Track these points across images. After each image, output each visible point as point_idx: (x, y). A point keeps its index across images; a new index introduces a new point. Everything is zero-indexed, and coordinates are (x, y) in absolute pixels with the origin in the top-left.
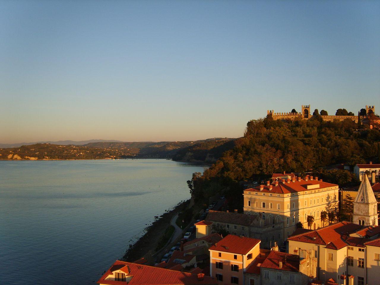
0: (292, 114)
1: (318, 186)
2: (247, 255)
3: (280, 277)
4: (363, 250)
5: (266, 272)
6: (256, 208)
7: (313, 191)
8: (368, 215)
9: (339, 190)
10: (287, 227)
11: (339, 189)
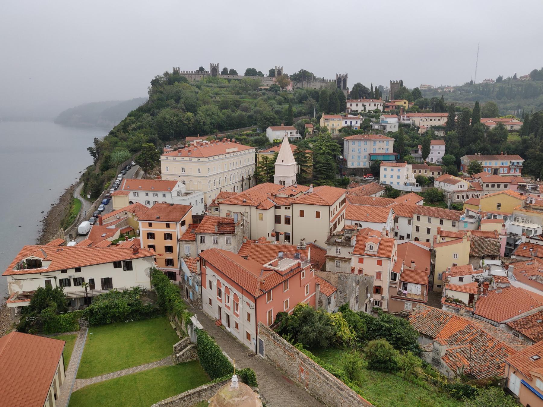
0: (200, 73)
1: (236, 149)
2: (180, 222)
4: (289, 208)
7: (232, 154)
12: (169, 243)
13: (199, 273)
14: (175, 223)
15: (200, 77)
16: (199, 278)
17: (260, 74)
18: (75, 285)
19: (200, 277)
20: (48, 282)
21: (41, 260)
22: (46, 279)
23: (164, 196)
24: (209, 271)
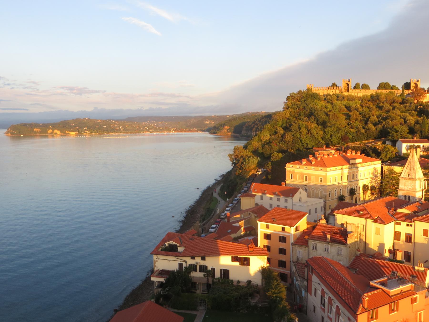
2: (295, 227)
3: (328, 249)
4: (411, 226)
5: (314, 244)
6: (298, 181)
8: (415, 191)
9: (381, 165)
10: (329, 200)
11: (382, 164)
12: (283, 245)
13: (306, 278)
14: (290, 227)
15: (332, 92)
16: (305, 283)
17: (394, 87)
18: (200, 271)
19: (307, 283)
20: (181, 265)
21: (178, 246)
22: (179, 262)
23: (286, 201)
24: (315, 279)
